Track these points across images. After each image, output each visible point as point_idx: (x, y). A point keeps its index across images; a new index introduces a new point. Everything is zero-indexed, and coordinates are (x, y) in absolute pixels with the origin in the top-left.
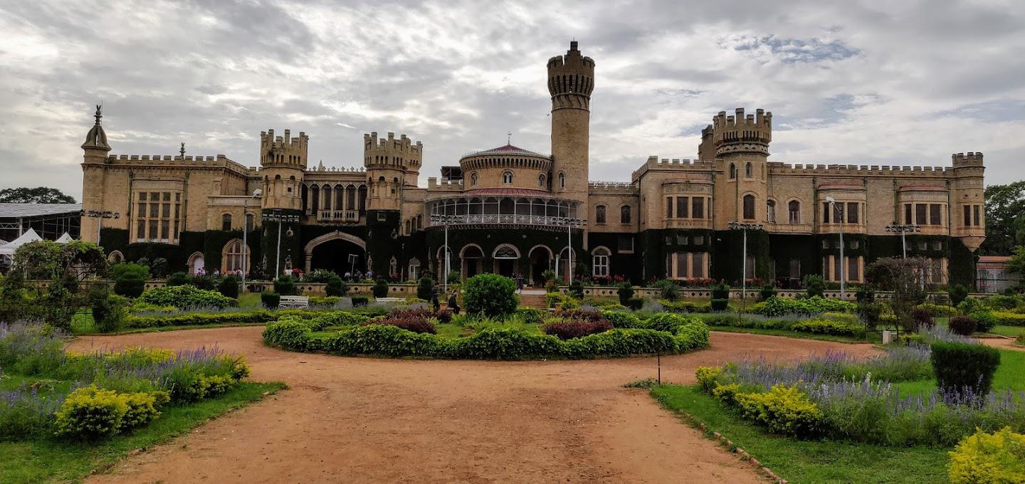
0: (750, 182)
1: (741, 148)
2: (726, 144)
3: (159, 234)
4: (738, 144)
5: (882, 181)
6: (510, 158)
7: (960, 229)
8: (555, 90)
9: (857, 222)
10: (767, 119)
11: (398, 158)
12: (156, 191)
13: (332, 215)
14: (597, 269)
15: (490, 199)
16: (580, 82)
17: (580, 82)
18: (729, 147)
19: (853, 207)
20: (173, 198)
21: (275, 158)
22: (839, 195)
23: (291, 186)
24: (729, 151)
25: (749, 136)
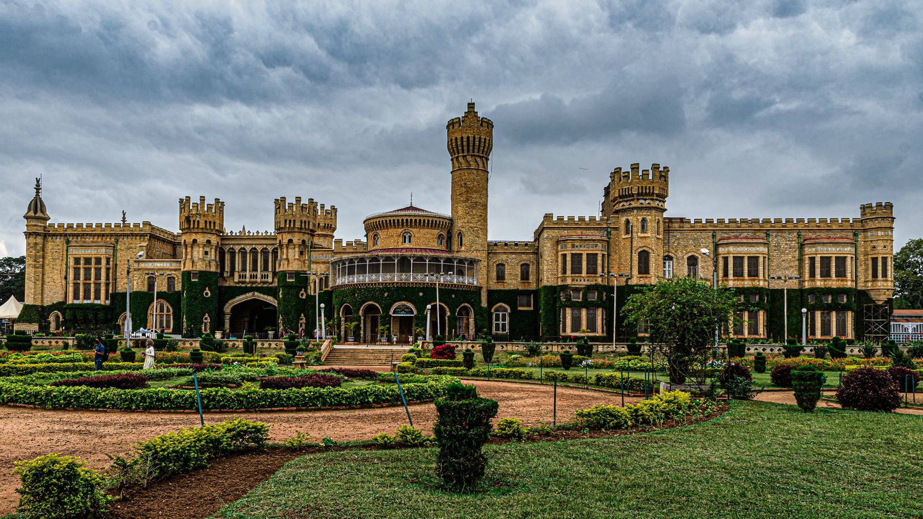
0: (645, 237)
1: (634, 204)
2: (621, 200)
3: (92, 296)
4: (633, 200)
5: (786, 235)
6: (409, 219)
7: (868, 281)
8: (454, 151)
9: (757, 275)
10: (663, 174)
11: (305, 221)
12: (88, 256)
13: (248, 276)
14: (497, 325)
15: (388, 258)
16: (477, 143)
17: (477, 143)
18: (625, 203)
19: (753, 260)
20: (104, 262)
21: (192, 223)
22: (739, 249)
23: (207, 249)
24: (624, 207)
25: (644, 192)
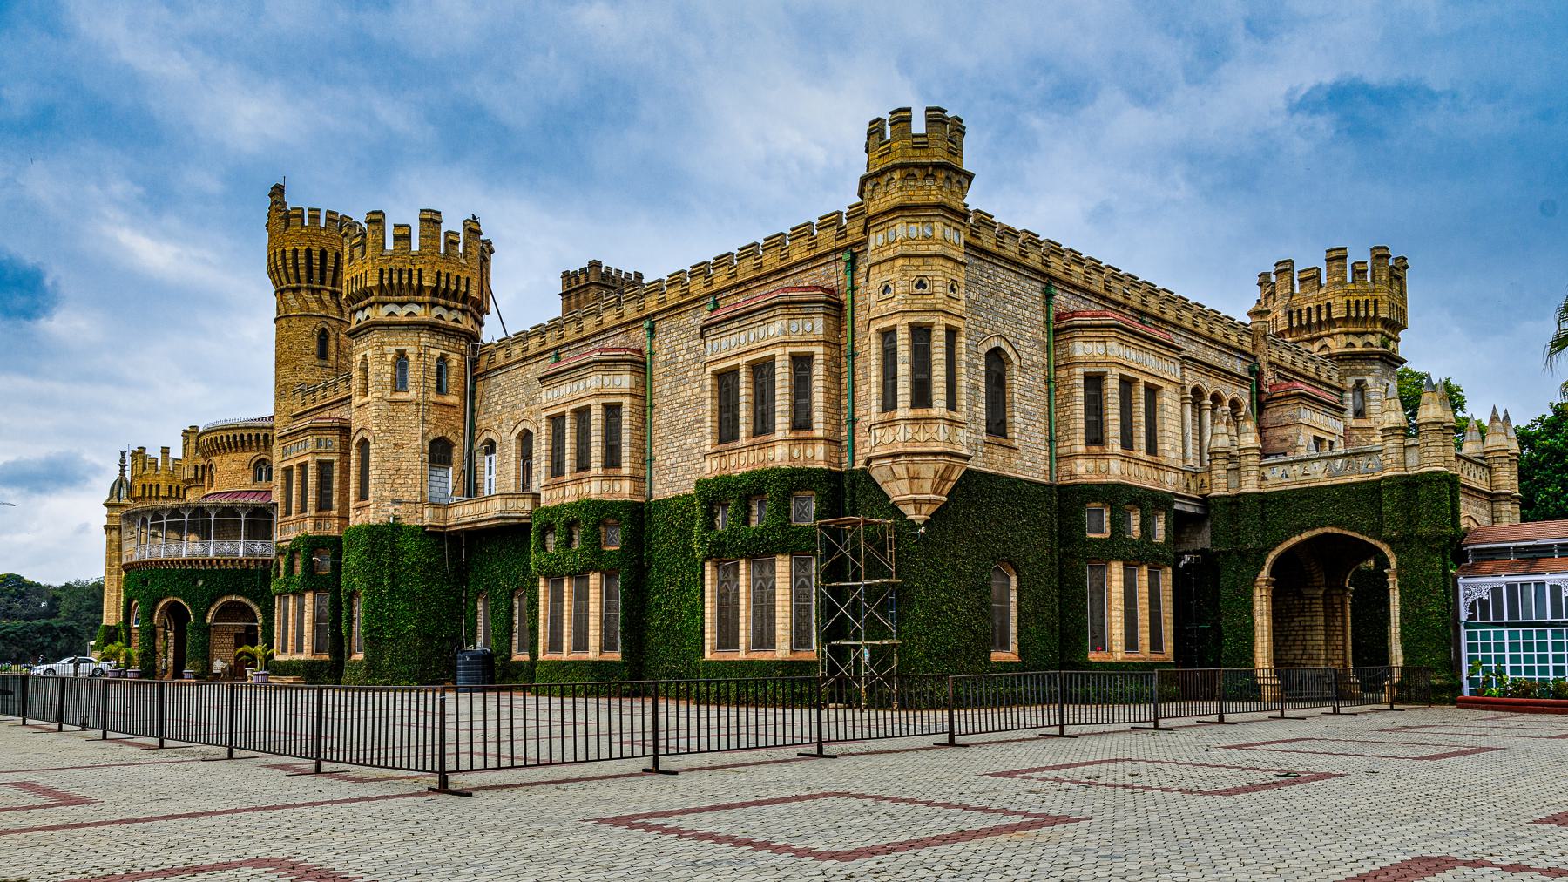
1: (421, 314)
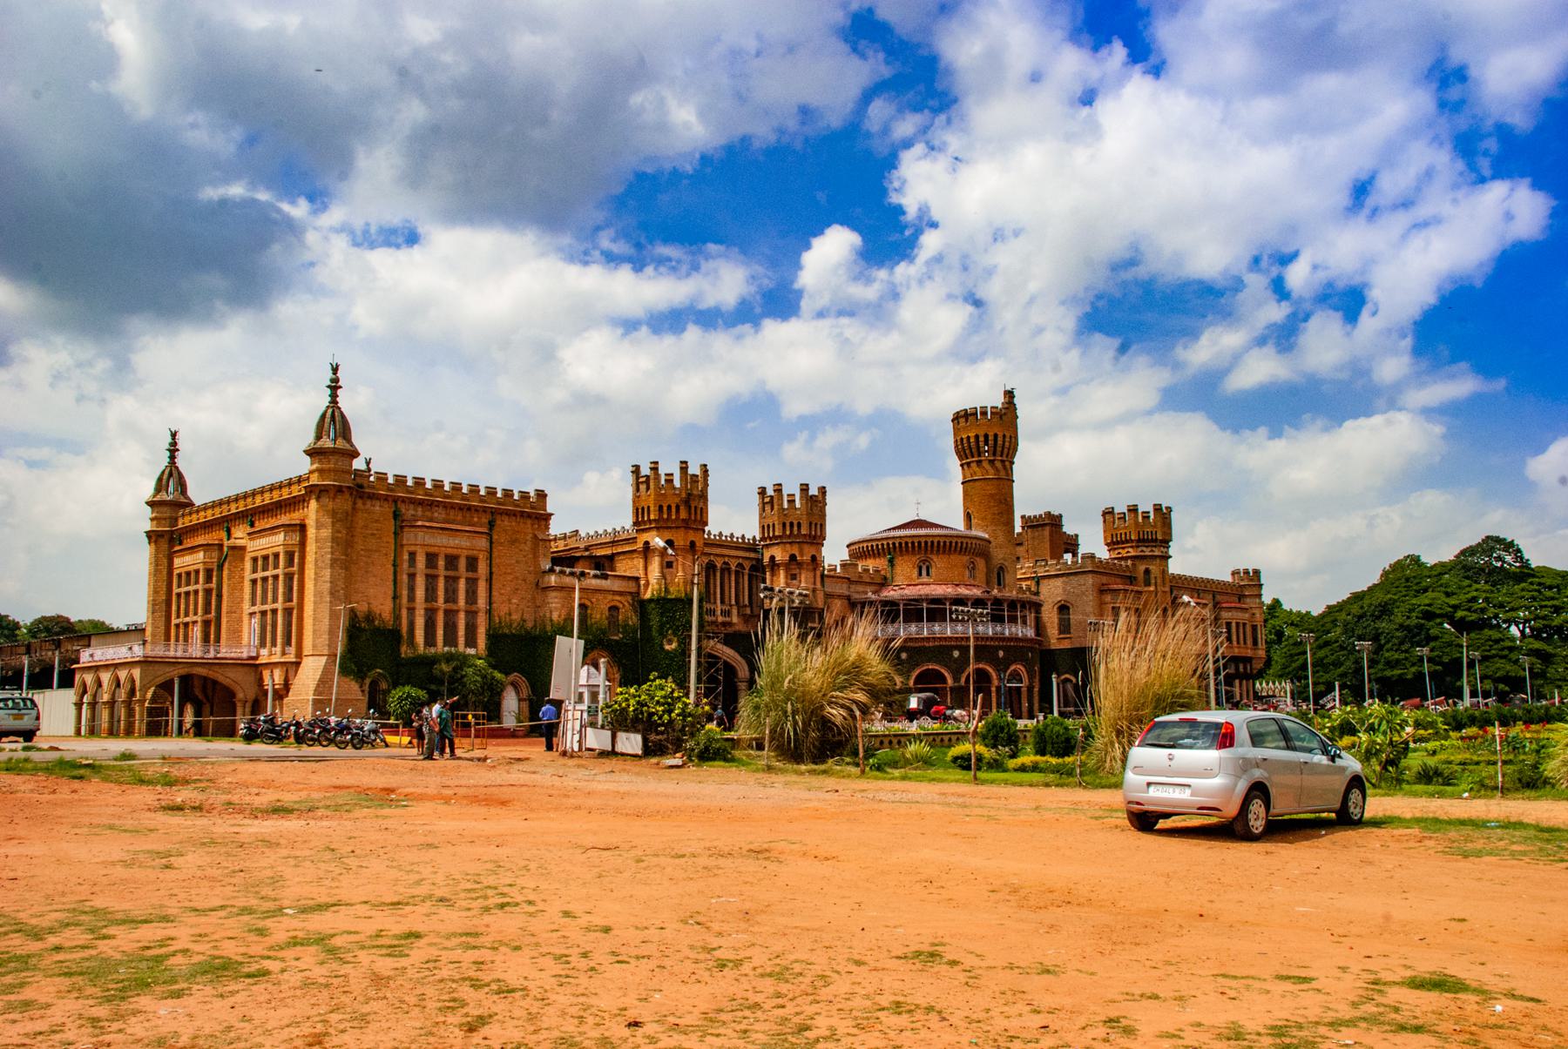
3: (461, 640)
12: (455, 552)
18: (1144, 549)
